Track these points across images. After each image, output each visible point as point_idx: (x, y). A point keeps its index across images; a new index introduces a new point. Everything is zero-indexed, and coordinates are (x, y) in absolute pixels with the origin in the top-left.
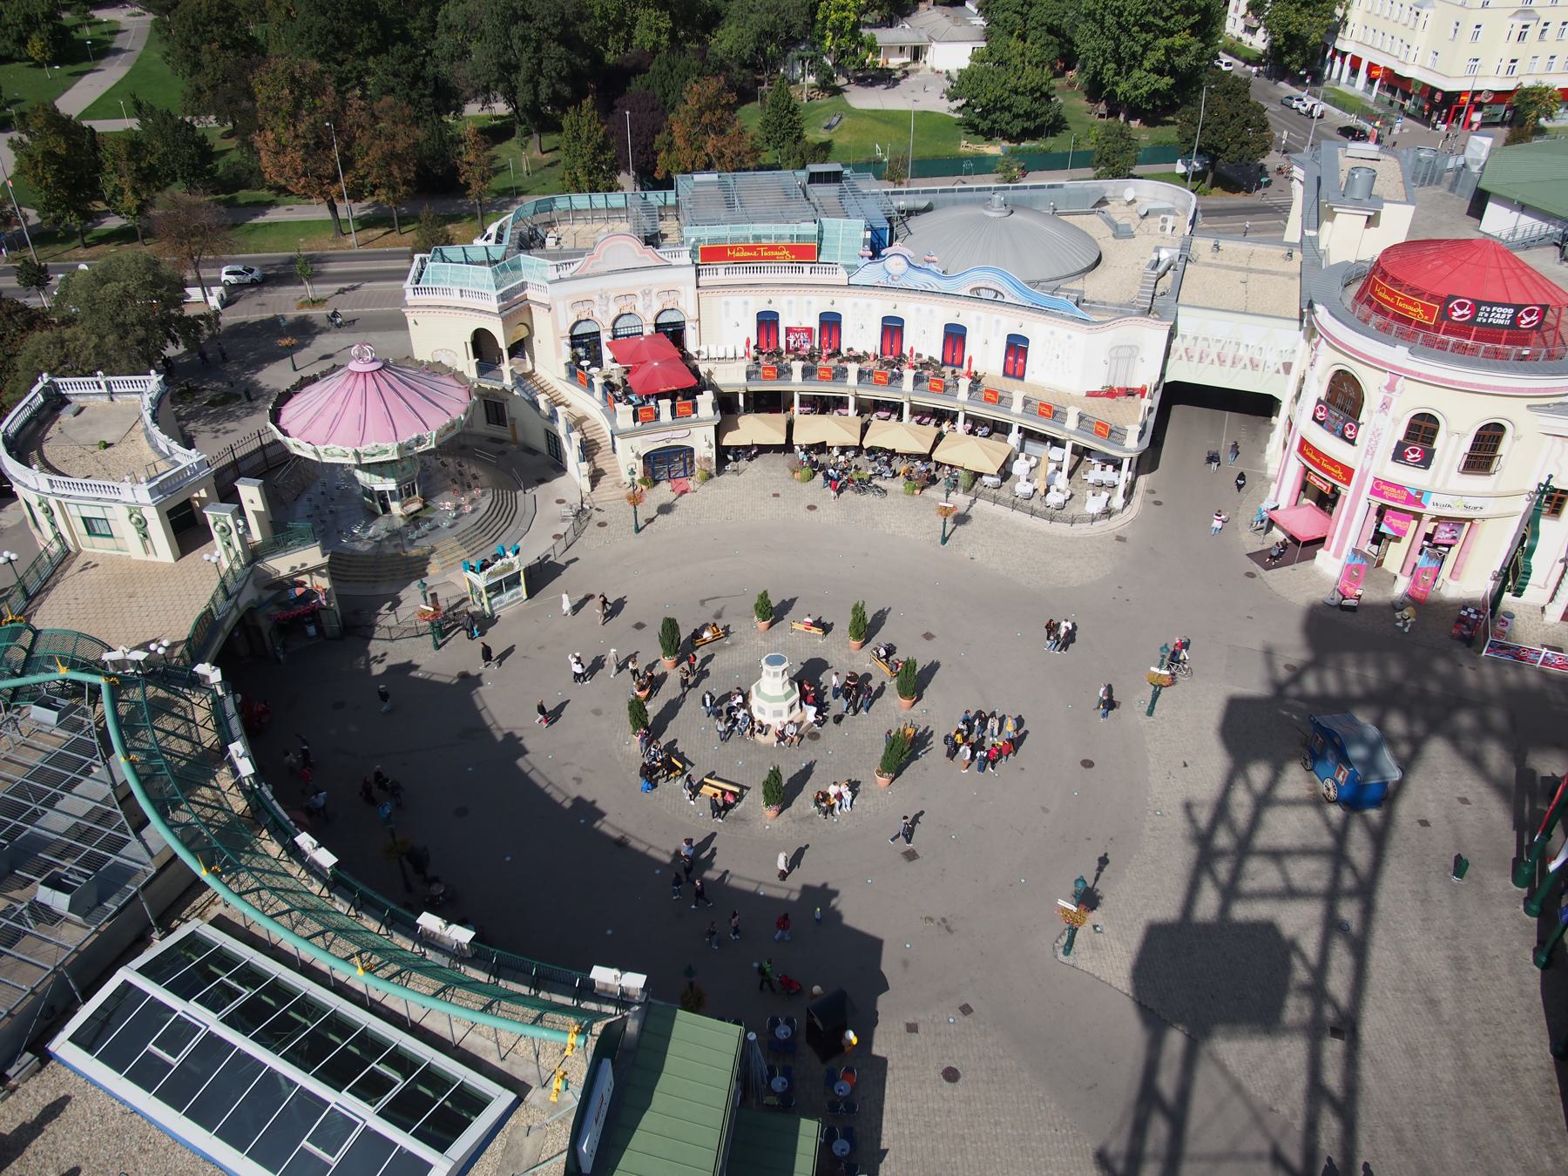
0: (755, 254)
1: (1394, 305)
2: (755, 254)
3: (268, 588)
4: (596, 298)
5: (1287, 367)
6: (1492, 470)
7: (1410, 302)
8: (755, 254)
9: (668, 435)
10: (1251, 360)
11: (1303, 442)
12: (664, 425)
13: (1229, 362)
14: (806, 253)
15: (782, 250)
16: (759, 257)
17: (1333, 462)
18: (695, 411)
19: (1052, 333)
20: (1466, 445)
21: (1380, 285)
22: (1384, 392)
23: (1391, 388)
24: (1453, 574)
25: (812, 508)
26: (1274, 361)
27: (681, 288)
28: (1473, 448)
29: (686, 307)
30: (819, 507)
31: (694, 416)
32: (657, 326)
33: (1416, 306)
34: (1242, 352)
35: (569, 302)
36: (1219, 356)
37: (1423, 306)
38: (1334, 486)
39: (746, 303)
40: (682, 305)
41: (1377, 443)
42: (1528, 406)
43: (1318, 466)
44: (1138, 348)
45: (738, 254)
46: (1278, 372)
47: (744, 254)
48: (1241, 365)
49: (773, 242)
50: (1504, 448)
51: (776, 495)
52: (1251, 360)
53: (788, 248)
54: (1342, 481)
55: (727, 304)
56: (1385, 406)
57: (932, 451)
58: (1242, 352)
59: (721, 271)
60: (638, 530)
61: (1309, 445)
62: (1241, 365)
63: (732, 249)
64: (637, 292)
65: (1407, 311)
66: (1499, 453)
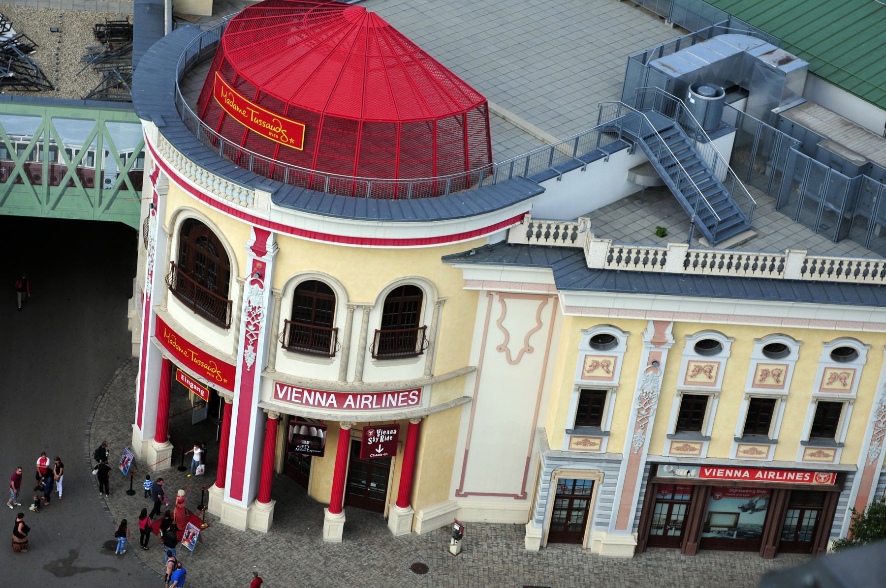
1: (247, 121)
5: (137, 179)
6: (418, 348)
7: (268, 118)
10: (79, 172)
13: (45, 178)
17: (204, 356)
20: (376, 322)
21: (226, 89)
22: (254, 256)
23: (259, 249)
24: (405, 499)
28: (386, 320)
33: (276, 125)
34: (62, 161)
36: (27, 167)
37: (286, 125)
38: (214, 393)
41: (257, 327)
42: (445, 259)
46: (123, 187)
48: (65, 181)
50: (426, 318)
52: (79, 172)
54: (222, 384)
56: (259, 272)
58: (62, 161)
61: (170, 331)
62: (65, 181)
65: (266, 131)
66: (421, 325)
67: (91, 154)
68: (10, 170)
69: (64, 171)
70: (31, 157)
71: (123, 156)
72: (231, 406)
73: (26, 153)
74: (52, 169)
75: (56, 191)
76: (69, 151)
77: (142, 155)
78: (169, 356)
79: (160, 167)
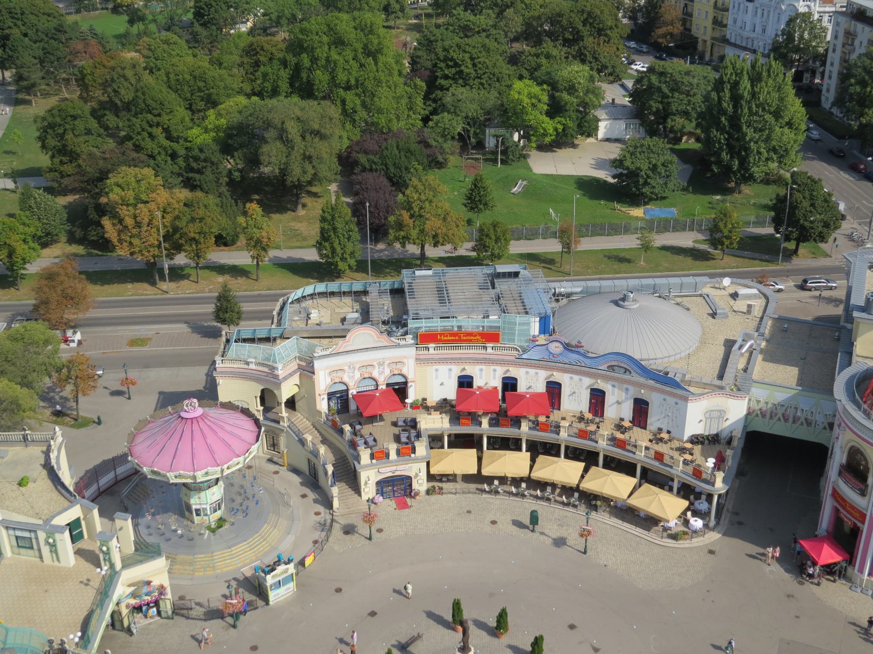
0: (458, 338)
2: (457, 338)
3: (130, 586)
4: (346, 368)
5: (831, 426)
8: (457, 338)
9: (394, 468)
10: (806, 419)
11: (835, 491)
12: (392, 462)
13: (791, 420)
14: (491, 337)
15: (475, 336)
16: (461, 341)
17: (853, 508)
18: (414, 453)
19: (665, 400)
25: (494, 522)
26: (820, 419)
27: (405, 360)
29: (410, 370)
30: (499, 523)
31: (413, 455)
32: (388, 385)
34: (799, 414)
35: (327, 371)
36: (783, 415)
38: (855, 524)
39: (450, 370)
40: (405, 371)
43: (844, 508)
44: (725, 412)
45: (445, 338)
46: (825, 428)
47: (449, 338)
48: (799, 423)
49: (470, 330)
51: (469, 512)
52: (806, 419)
53: (480, 334)
54: (859, 521)
55: (437, 370)
57: (580, 482)
58: (799, 414)
59: (432, 351)
60: (370, 539)
61: (838, 494)
62: (799, 423)
63: (441, 335)
64: (375, 363)
67: (812, 413)
68: (776, 415)
69: (799, 419)
70: (786, 410)
71: (826, 415)
72: (862, 531)
73: (784, 408)
74: (794, 417)
75: (795, 426)
76: (802, 410)
77: (835, 416)
78: (836, 504)
79: (843, 423)
